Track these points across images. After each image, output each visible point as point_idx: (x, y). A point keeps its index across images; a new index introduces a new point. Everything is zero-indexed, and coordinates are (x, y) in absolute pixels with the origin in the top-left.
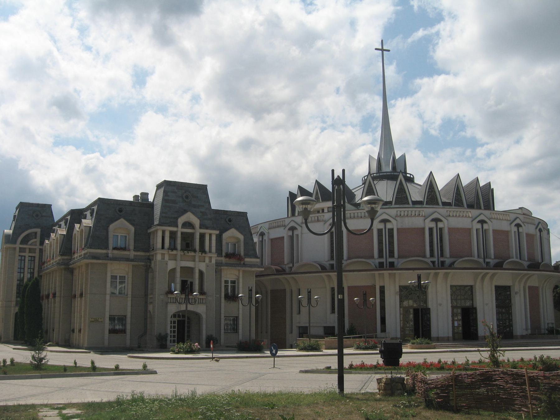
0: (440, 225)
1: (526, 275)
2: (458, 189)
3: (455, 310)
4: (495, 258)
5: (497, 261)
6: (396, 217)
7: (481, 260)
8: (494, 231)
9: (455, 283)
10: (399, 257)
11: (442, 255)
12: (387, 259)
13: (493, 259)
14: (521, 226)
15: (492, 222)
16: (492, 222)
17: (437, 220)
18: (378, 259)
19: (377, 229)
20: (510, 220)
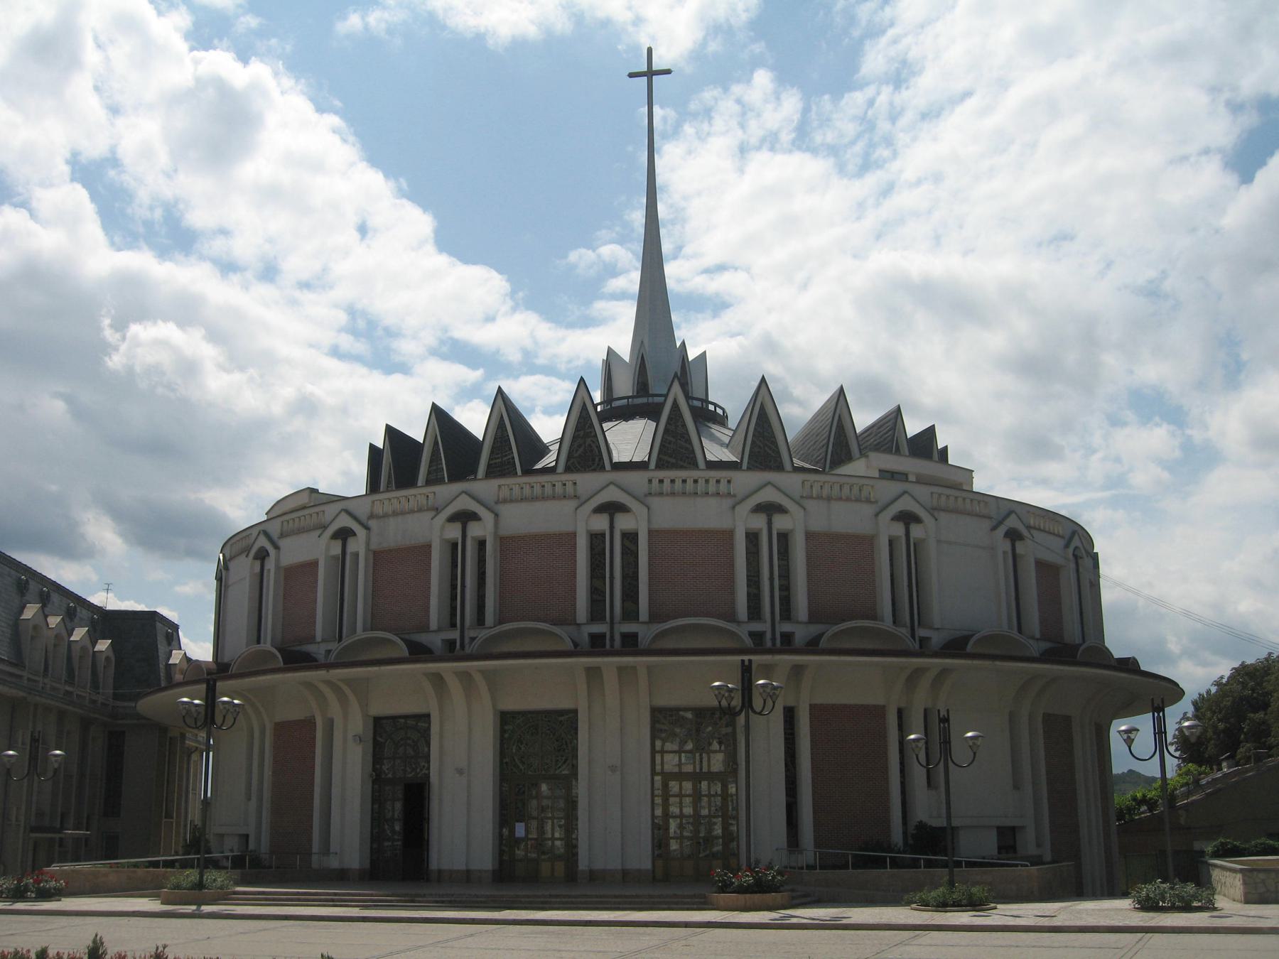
0: (624, 523)
1: (918, 673)
2: (841, 427)
3: (674, 786)
4: (814, 617)
5: (815, 629)
6: (497, 502)
7: (904, 632)
8: (810, 536)
9: (663, 701)
10: (501, 621)
11: (630, 614)
12: (466, 632)
13: (801, 623)
14: (918, 520)
15: (805, 509)
16: (805, 509)
17: (612, 509)
18: (440, 630)
19: (447, 541)
20: (876, 502)
